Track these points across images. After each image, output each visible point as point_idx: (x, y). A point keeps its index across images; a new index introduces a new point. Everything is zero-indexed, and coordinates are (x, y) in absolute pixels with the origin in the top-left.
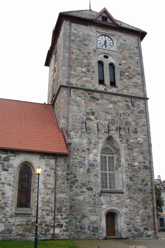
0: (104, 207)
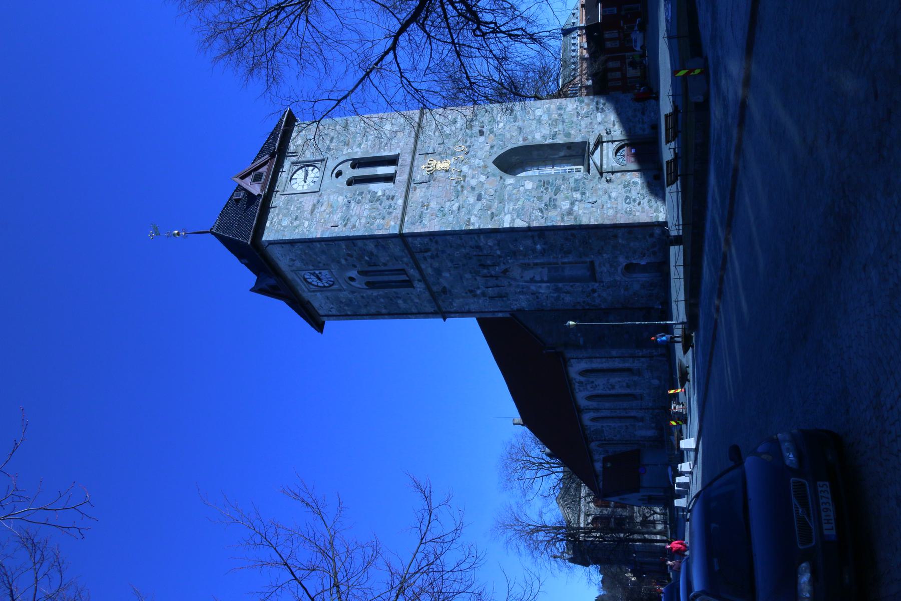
0: (618, 278)
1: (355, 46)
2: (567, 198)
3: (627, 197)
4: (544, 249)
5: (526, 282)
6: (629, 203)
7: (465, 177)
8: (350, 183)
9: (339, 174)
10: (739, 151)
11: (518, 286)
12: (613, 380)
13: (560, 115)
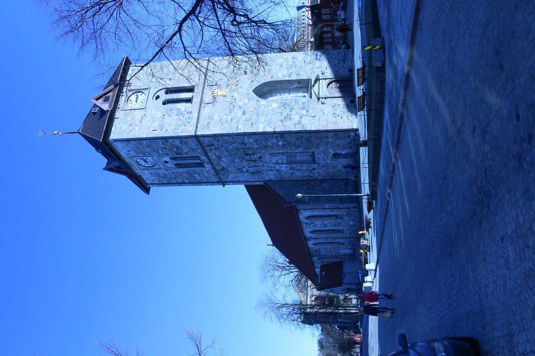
0: (329, 162)
1: (155, 28)
2: (298, 113)
3: (334, 113)
4: (284, 145)
5: (273, 164)
7: (235, 100)
8: (164, 103)
9: (158, 97)
10: (404, 104)
11: (268, 166)
12: (325, 222)
13: (294, 62)
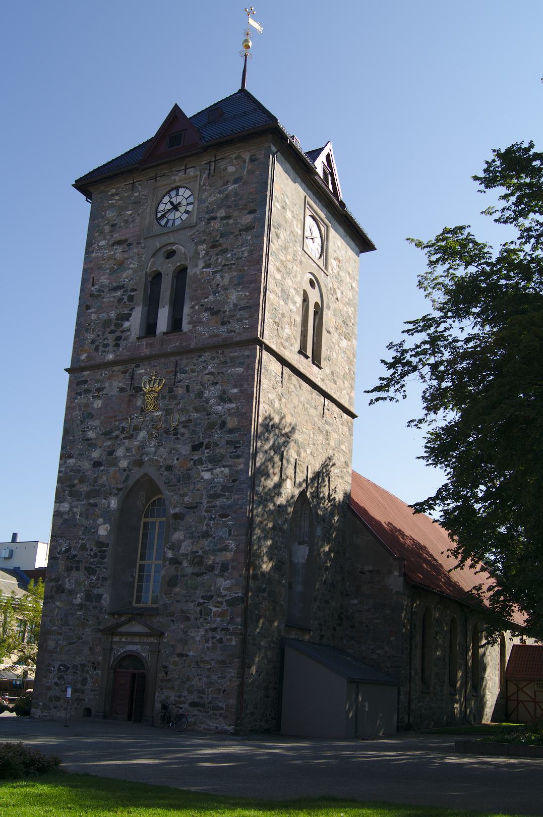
6: (59, 669)
13: (211, 568)
